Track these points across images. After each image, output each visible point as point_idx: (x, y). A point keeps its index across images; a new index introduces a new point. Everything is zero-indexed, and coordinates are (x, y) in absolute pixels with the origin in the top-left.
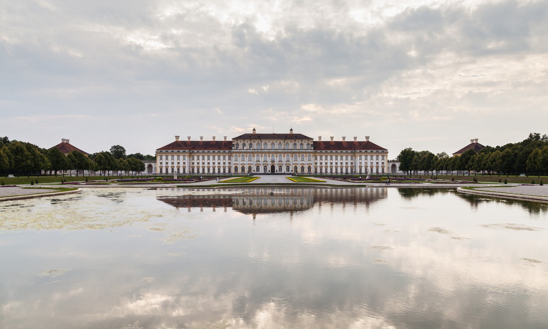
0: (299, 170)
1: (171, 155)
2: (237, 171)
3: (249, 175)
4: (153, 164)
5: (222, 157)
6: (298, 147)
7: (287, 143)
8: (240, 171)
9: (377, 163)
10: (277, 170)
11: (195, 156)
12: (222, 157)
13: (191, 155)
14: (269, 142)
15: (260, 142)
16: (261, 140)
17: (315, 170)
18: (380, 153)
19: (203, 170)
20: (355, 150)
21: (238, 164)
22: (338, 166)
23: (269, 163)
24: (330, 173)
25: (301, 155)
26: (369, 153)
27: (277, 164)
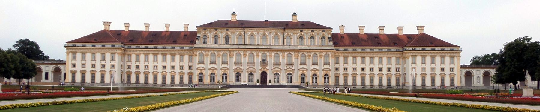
0: (309, 79)
1: (91, 52)
2: (203, 81)
3: (220, 87)
4: (61, 67)
5: (177, 57)
6: (307, 41)
7: (289, 36)
8: (207, 80)
9: (442, 69)
10: (270, 81)
11: (132, 54)
12: (177, 57)
13: (126, 52)
14: (258, 33)
15: (243, 33)
16: (244, 29)
17: (336, 80)
18: (447, 52)
19: (146, 78)
20: (403, 48)
21: (204, 69)
22: (383, 75)
24: (362, 85)
25: (312, 54)
26: (428, 52)
27: (270, 70)
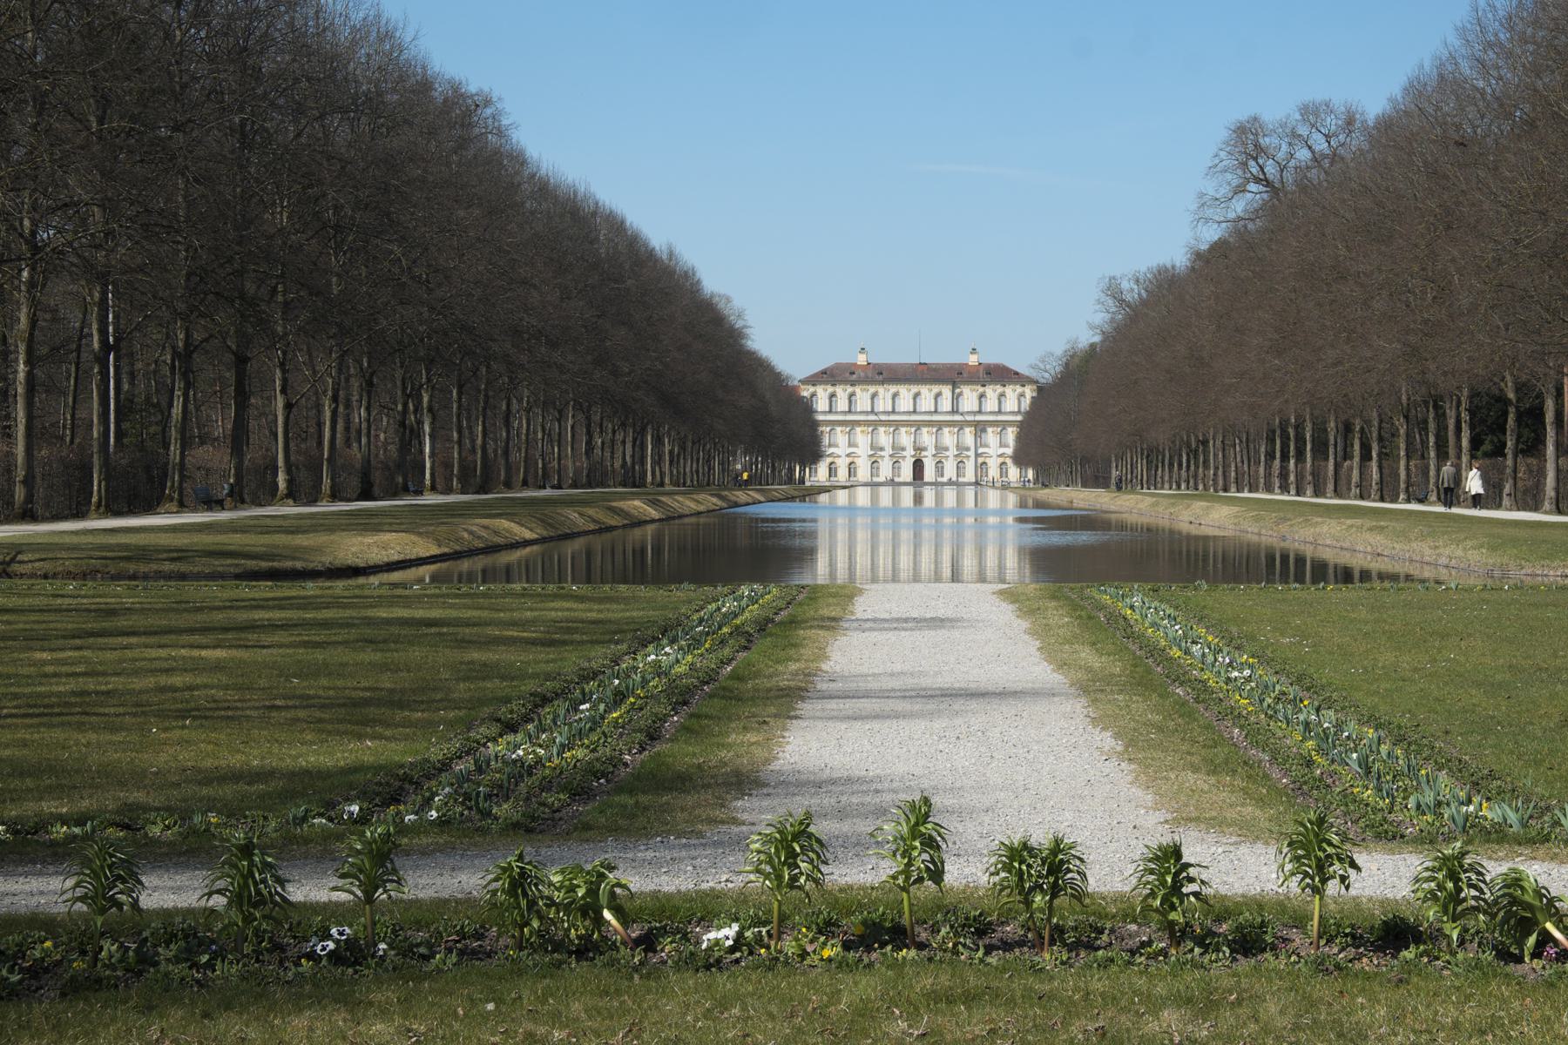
7: (960, 394)
23: (910, 452)
